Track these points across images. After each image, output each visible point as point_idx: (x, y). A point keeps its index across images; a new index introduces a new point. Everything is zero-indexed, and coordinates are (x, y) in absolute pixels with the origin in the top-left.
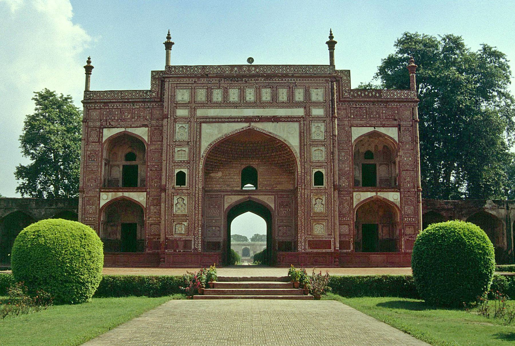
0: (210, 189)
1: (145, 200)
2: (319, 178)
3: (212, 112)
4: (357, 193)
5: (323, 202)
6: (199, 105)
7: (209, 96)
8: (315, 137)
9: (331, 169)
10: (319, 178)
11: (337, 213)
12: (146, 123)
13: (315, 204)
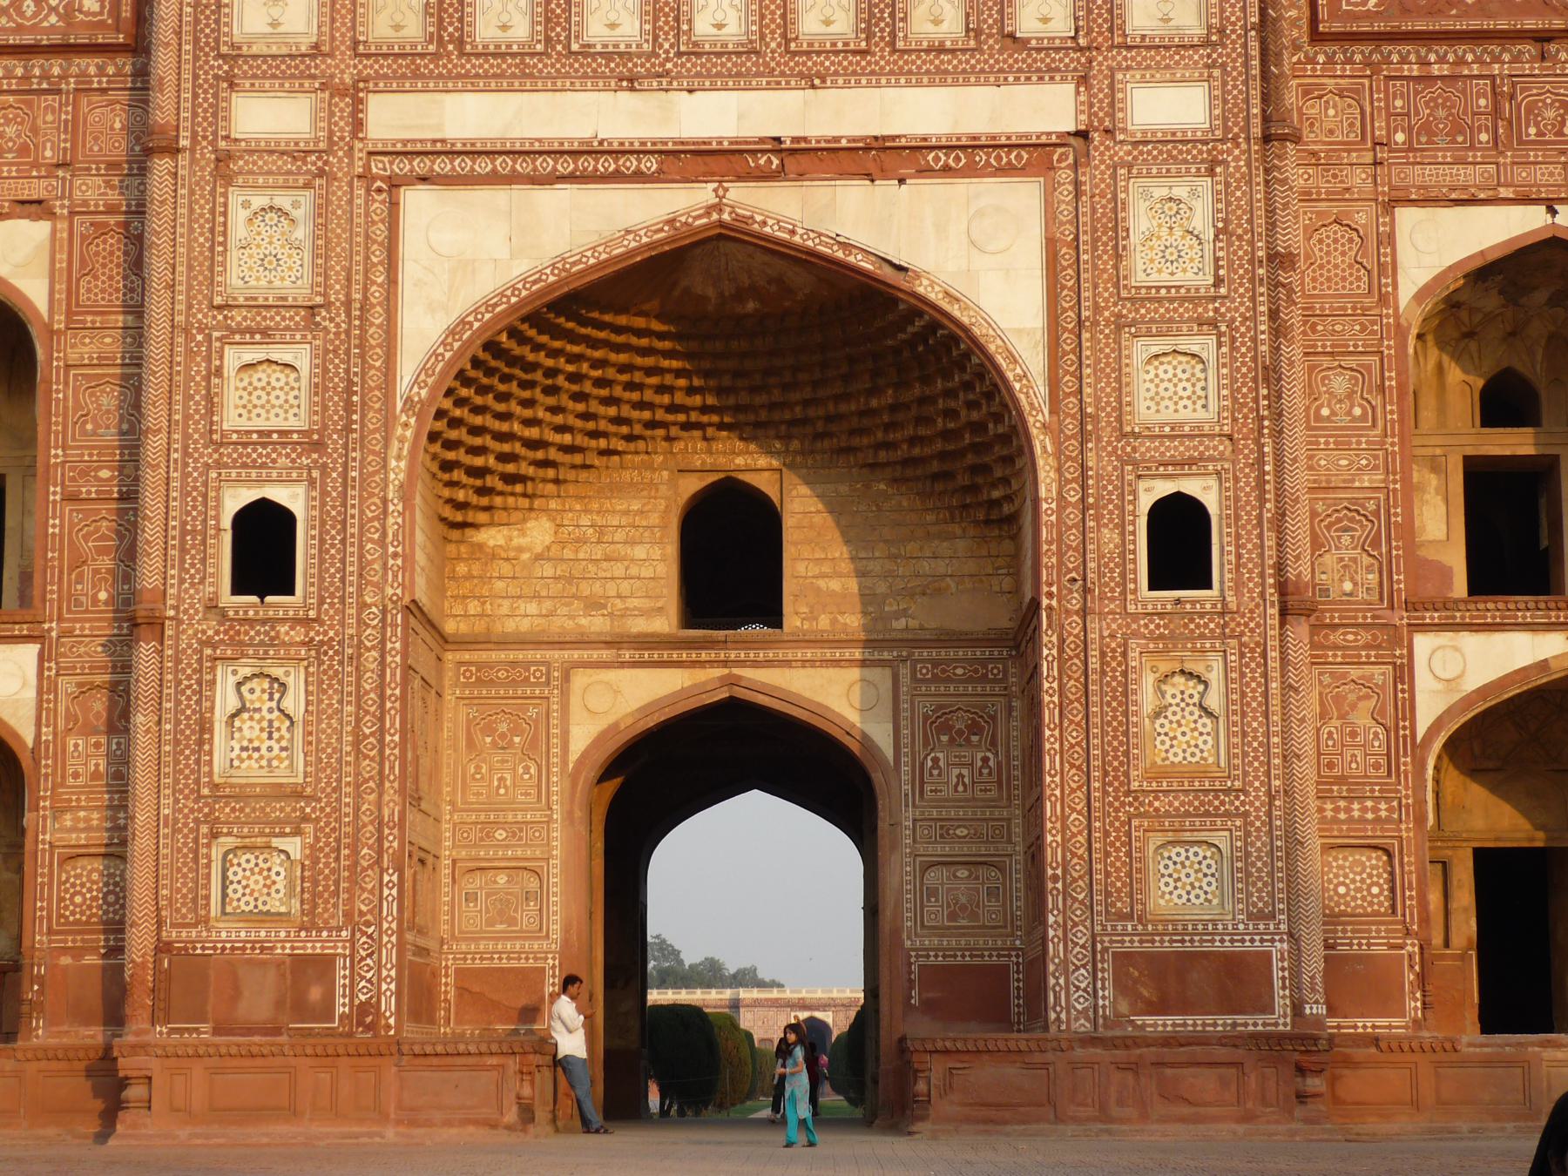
0: (480, 626)
1: (31, 693)
3: (470, 115)
4: (1445, 638)
5: (1214, 701)
6: (385, 66)
8: (1145, 269)
9: (1260, 483)
11: (1306, 770)
12: (36, 189)
13: (1157, 715)
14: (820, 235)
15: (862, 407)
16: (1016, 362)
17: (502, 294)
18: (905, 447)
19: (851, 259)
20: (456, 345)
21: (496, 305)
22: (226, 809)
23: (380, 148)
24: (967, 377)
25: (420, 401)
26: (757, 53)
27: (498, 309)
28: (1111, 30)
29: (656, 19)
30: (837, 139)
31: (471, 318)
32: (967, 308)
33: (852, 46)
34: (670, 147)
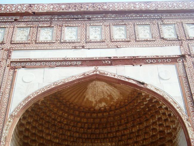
14: (122, 76)
15: (131, 132)
16: (176, 104)
17: (40, 90)
18: (141, 142)
19: (130, 81)
20: (26, 102)
21: (38, 93)
23: (14, 60)
24: (160, 116)
25: (15, 116)
26: (104, 42)
27: (39, 94)
28: (186, 36)
29: (81, 36)
30: (125, 57)
31: (31, 96)
32: (161, 92)
33: (126, 40)
34: (84, 59)
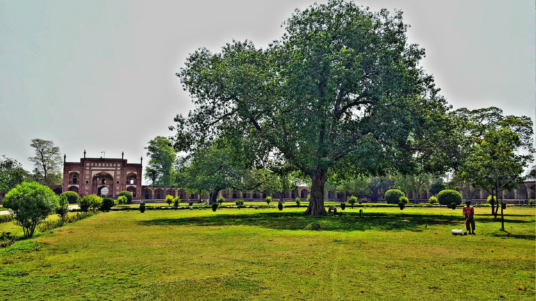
2: (118, 182)
7: (94, 164)
10: (118, 182)
22: (85, 190)
